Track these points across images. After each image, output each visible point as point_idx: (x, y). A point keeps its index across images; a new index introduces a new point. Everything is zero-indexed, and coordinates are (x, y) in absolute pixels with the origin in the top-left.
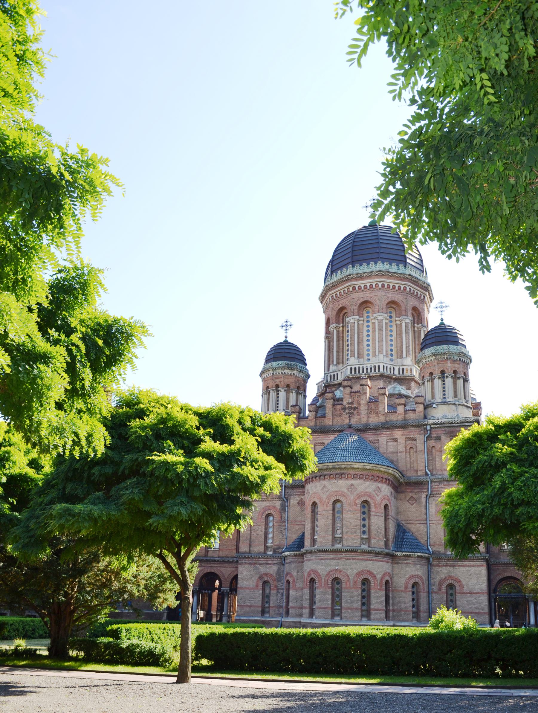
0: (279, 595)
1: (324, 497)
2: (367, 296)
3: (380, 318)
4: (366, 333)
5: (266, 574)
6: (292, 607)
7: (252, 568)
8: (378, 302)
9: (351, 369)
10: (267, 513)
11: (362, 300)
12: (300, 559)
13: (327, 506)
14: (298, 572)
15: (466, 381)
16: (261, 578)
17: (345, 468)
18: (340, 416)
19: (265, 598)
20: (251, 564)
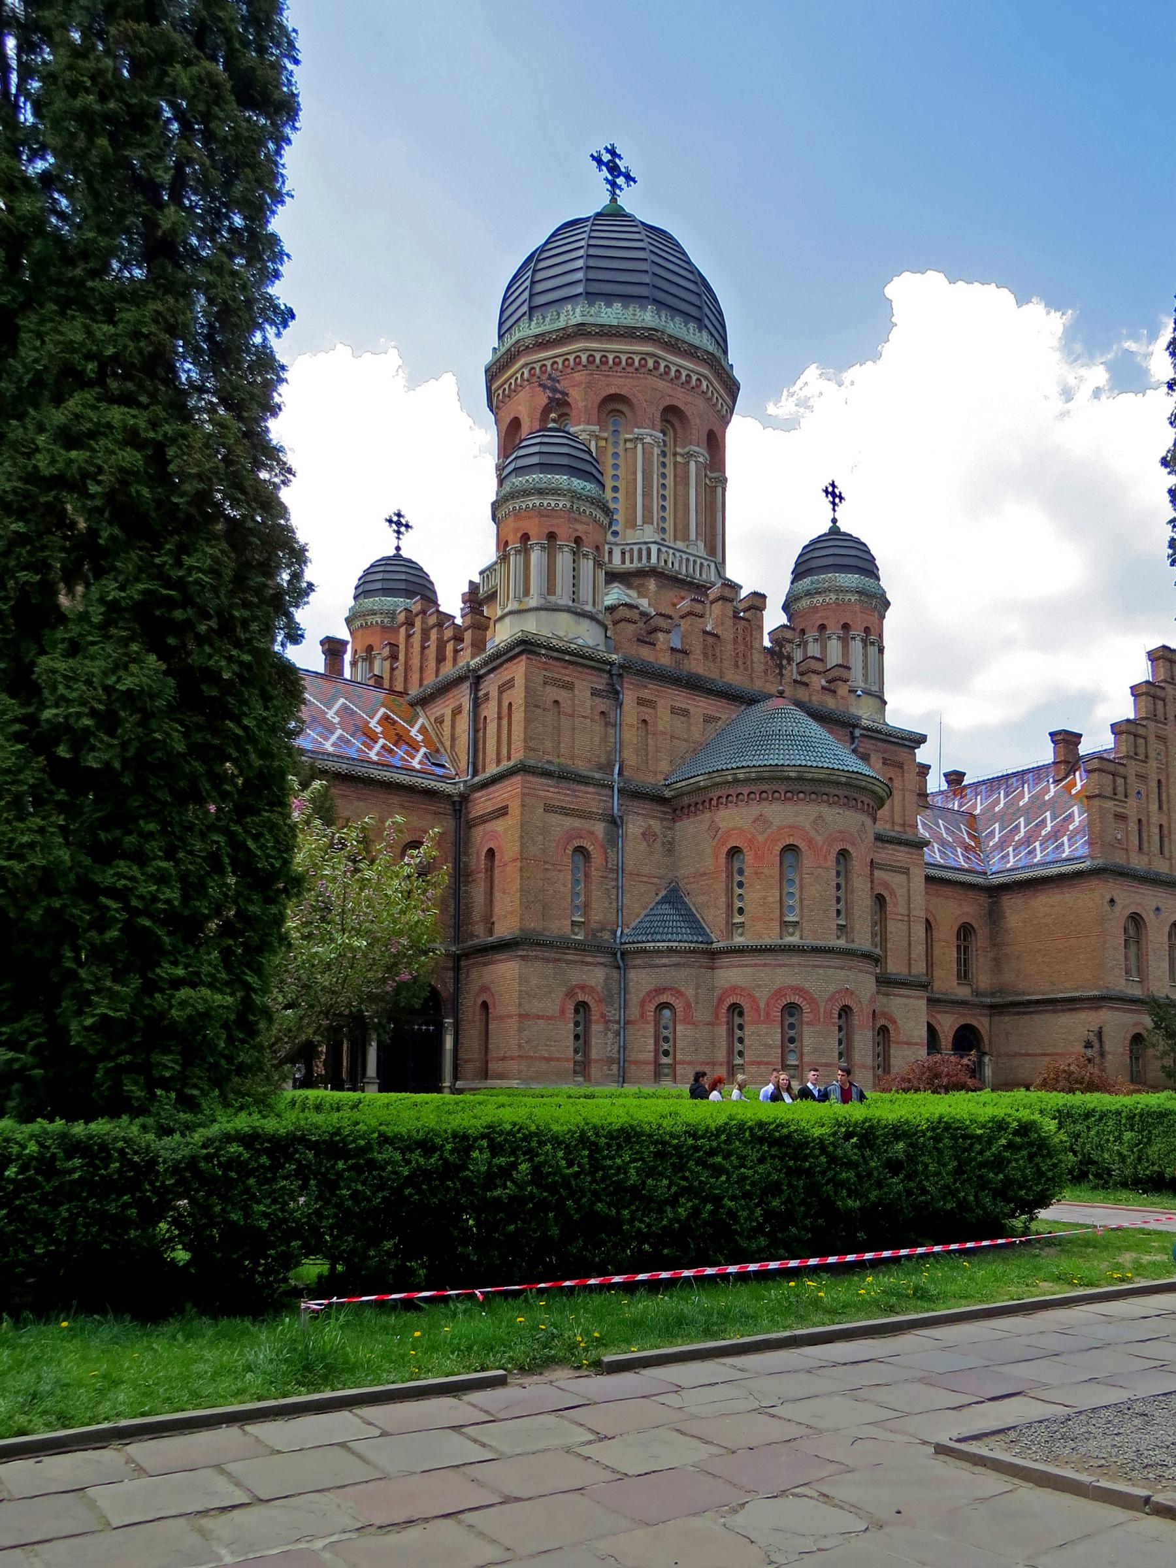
0: (610, 1035)
1: (819, 840)
2: (680, 398)
3: (701, 459)
4: (621, 472)
5: (582, 988)
6: (683, 1063)
7: (549, 969)
8: (698, 421)
9: (659, 550)
10: (576, 843)
11: (668, 402)
12: (704, 961)
13: (825, 859)
14: (698, 987)
15: (881, 650)
16: (570, 994)
17: (864, 789)
18: (714, 661)
19: (582, 1039)
20: (548, 960)
